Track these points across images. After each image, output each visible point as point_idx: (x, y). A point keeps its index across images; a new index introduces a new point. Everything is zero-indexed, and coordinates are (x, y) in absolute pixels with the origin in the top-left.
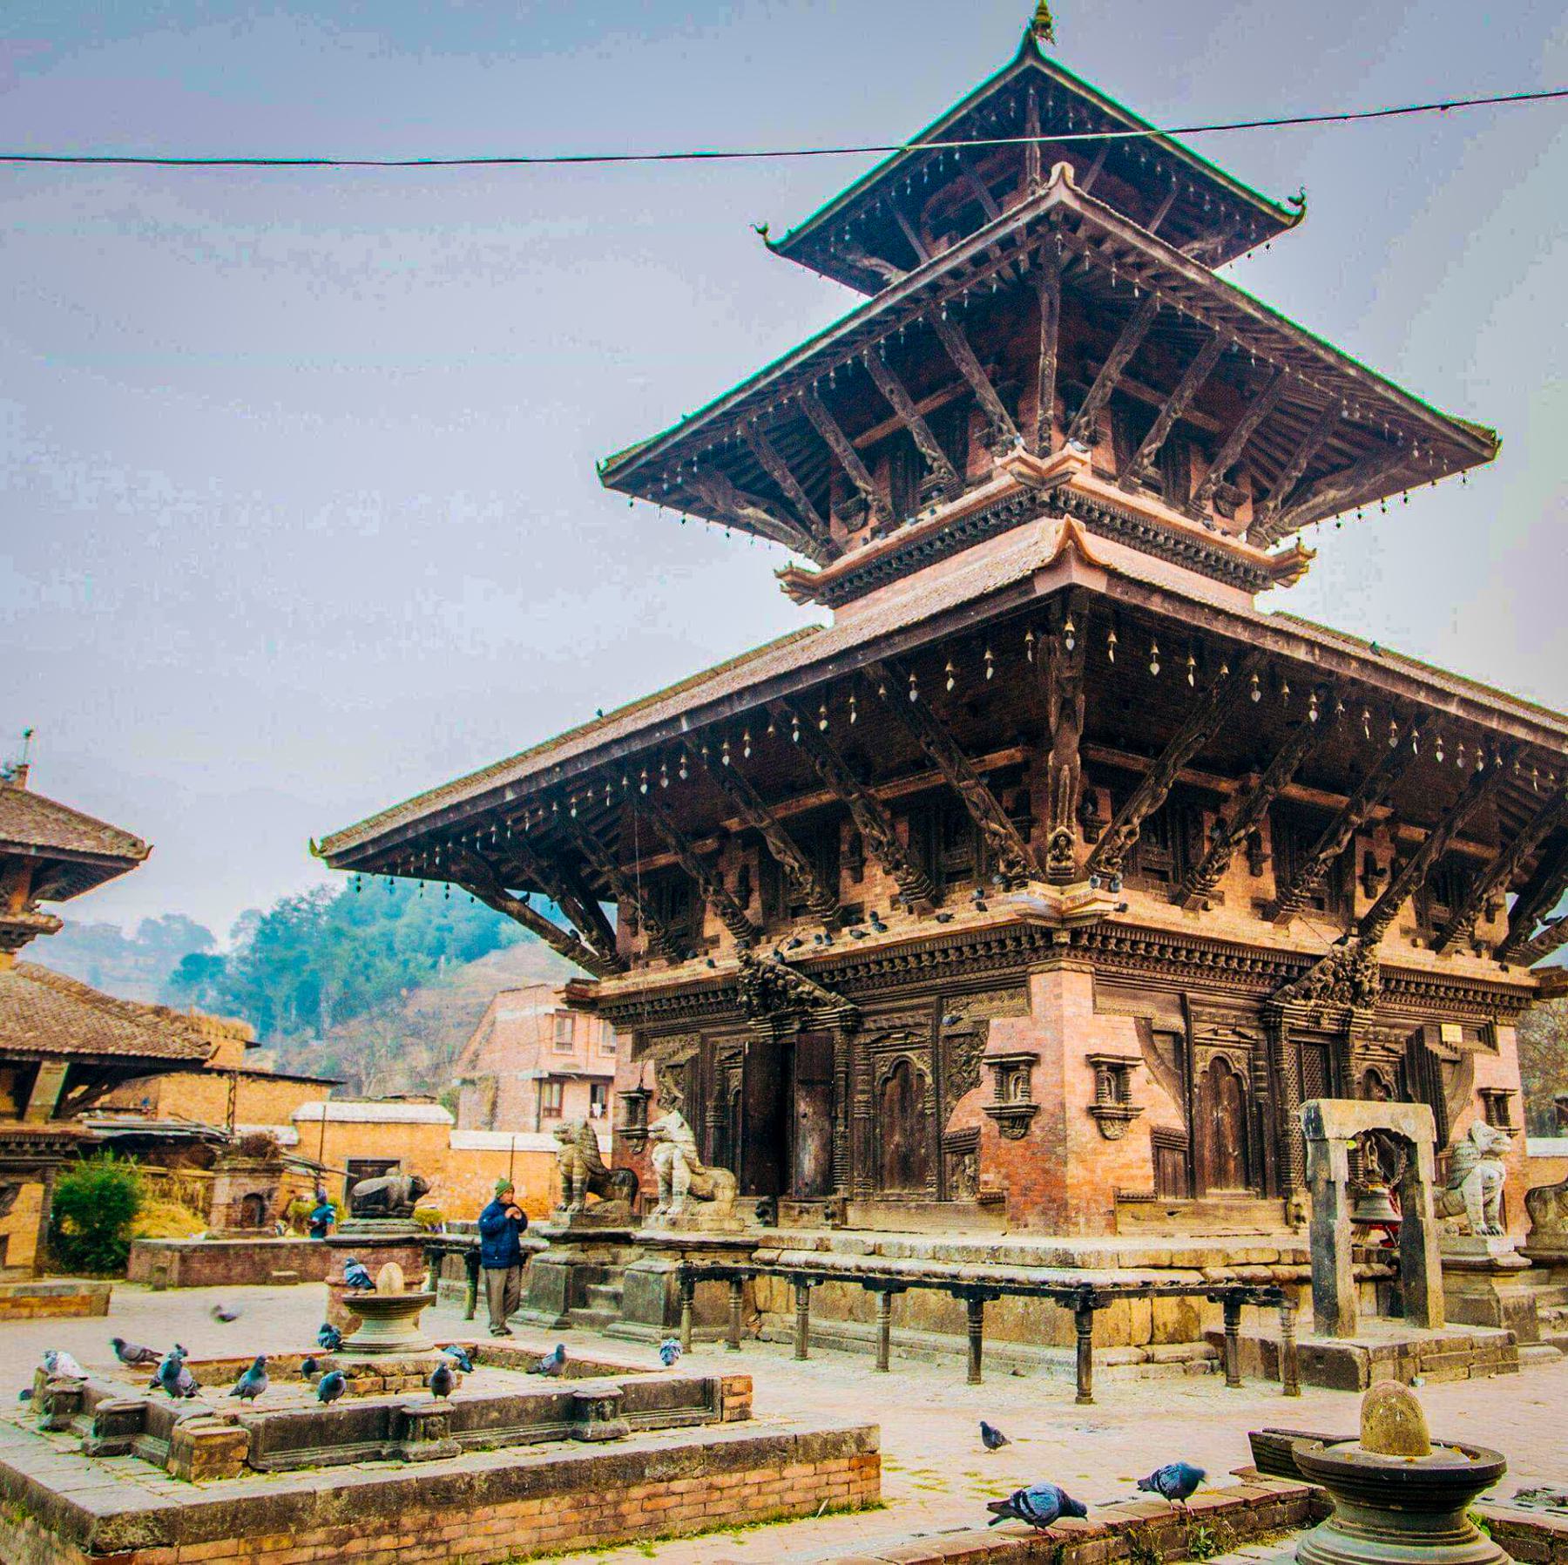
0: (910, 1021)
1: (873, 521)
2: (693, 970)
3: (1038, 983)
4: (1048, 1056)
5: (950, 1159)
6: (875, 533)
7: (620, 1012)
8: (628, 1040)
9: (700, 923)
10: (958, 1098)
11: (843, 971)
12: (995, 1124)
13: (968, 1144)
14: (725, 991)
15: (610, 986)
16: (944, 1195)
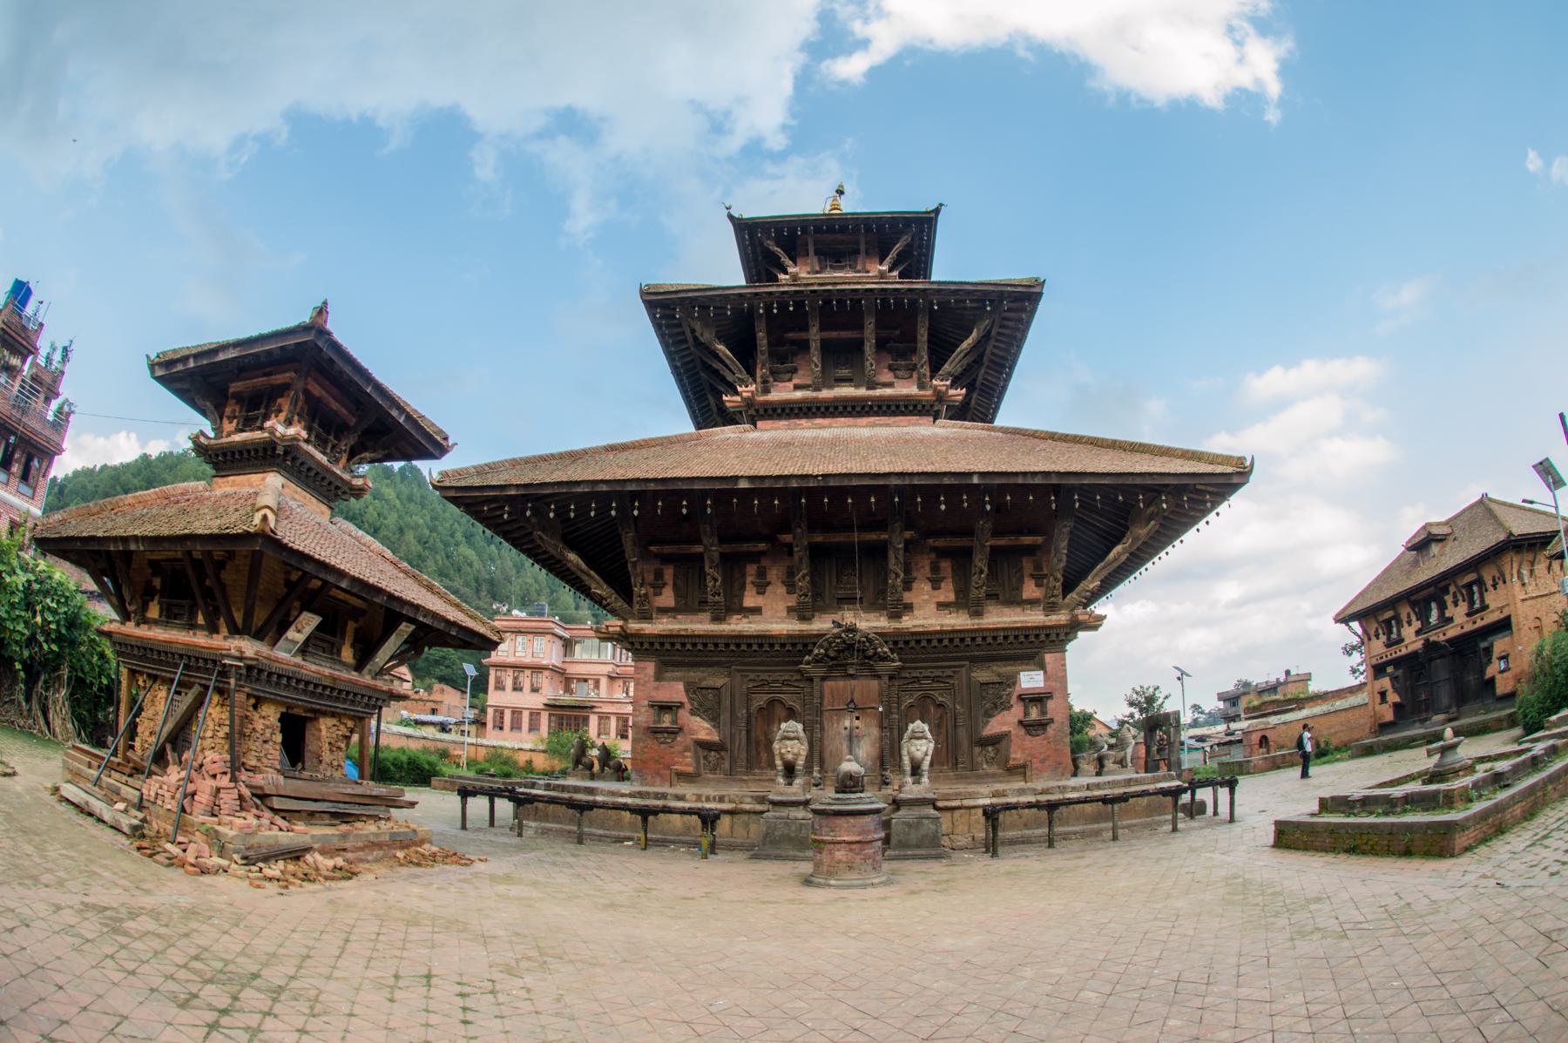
0: (938, 673)
1: (796, 381)
2: (738, 625)
3: (1049, 658)
4: (1057, 695)
5: (977, 750)
6: (797, 387)
7: (637, 645)
8: (650, 667)
9: (741, 597)
10: (991, 716)
11: (907, 642)
12: (1022, 732)
13: (996, 740)
14: (783, 645)
15: (648, 628)
16: (973, 767)
